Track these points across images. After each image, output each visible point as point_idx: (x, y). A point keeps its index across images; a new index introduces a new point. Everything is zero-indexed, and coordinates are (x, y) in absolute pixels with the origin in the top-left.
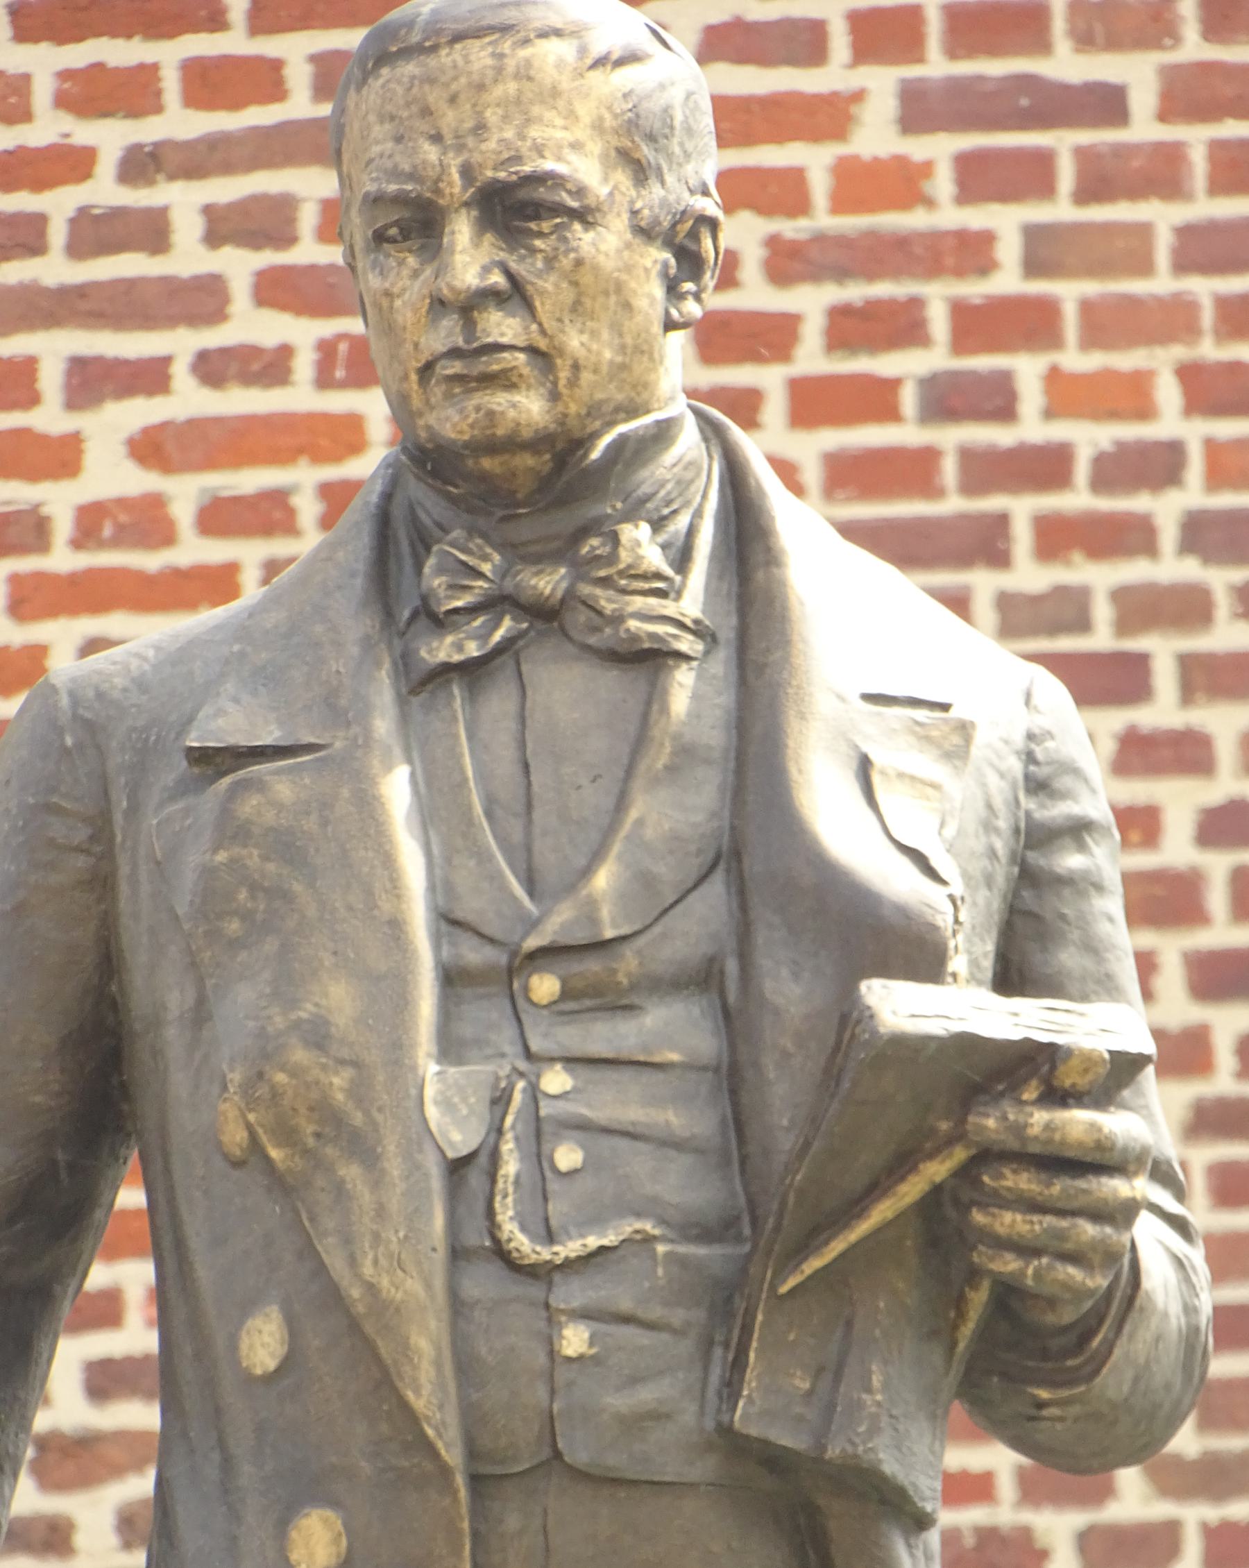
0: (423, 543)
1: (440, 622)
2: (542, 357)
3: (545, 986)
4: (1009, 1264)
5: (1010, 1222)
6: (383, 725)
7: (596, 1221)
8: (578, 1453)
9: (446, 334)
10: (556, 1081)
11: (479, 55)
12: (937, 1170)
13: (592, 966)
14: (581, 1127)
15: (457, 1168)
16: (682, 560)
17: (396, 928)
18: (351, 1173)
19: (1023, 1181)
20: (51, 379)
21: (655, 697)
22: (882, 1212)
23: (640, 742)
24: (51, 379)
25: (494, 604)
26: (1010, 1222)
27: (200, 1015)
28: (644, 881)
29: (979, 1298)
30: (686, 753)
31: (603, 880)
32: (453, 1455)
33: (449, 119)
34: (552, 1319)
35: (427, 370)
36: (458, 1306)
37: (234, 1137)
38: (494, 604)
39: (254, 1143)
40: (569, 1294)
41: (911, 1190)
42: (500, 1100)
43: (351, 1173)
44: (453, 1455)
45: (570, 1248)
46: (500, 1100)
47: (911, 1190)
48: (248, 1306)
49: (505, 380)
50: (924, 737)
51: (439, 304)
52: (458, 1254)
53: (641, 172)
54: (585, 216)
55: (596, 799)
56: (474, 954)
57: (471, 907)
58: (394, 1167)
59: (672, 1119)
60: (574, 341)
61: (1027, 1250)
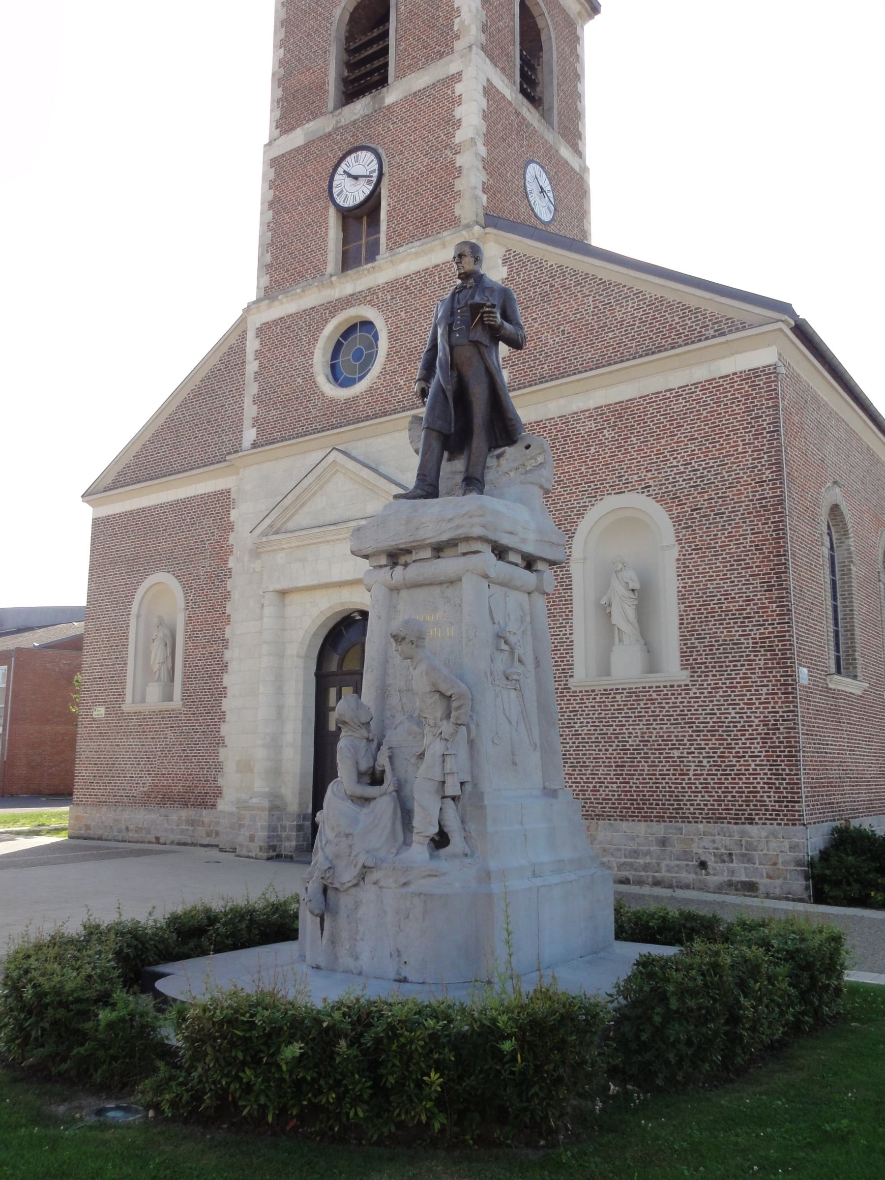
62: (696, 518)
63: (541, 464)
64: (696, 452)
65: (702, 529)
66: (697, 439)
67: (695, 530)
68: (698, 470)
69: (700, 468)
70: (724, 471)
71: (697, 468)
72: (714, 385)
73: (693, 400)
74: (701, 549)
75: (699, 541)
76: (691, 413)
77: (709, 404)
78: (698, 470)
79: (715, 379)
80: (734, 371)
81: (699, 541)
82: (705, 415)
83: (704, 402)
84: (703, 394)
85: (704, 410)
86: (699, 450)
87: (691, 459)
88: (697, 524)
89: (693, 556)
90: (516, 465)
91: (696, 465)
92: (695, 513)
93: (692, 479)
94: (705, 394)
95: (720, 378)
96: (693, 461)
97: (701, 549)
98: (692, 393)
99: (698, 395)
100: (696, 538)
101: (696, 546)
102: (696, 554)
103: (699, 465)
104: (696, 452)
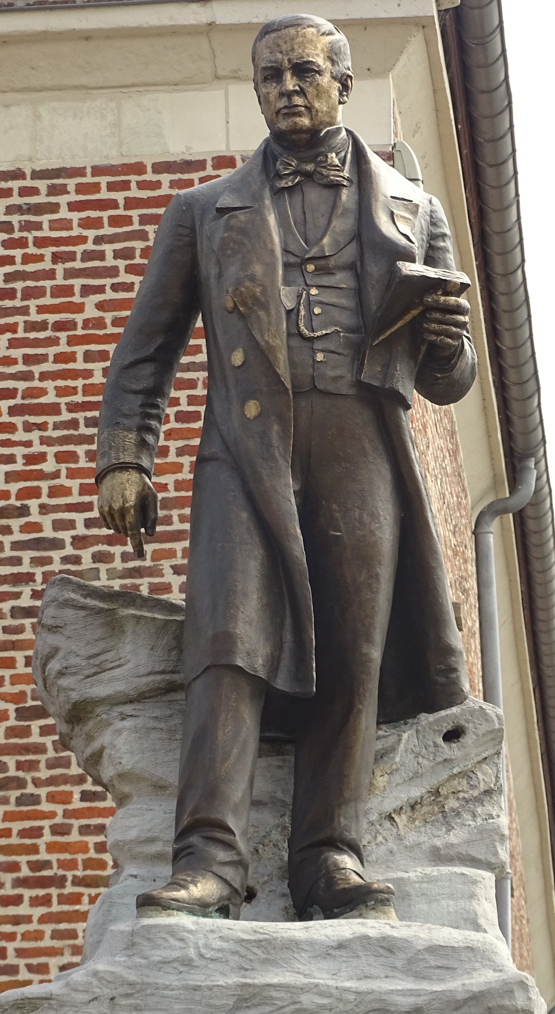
0: (275, 159)
1: (281, 177)
2: (309, 108)
3: (311, 267)
4: (434, 338)
5: (434, 326)
6: (268, 202)
7: (325, 328)
8: (320, 385)
9: (283, 102)
10: (314, 291)
11: (292, 31)
12: (415, 312)
13: (322, 262)
14: (321, 303)
15: (289, 312)
16: (343, 162)
17: (272, 252)
18: (262, 313)
19: (438, 315)
20: (77, 290)
21: (338, 196)
22: (400, 324)
23: (334, 207)
24: (77, 290)
25: (295, 173)
26: (434, 326)
27: (220, 276)
28: (335, 242)
29: (424, 348)
30: (346, 210)
31: (326, 241)
32: (289, 386)
33: (284, 47)
34: (314, 352)
35: (278, 112)
36: (289, 348)
37: (230, 305)
38: (295, 173)
39: (235, 306)
40: (318, 345)
41: (408, 318)
42: (300, 296)
43: (262, 313)
44: (289, 386)
45: (319, 334)
46: (300, 296)
47: (408, 318)
48: (233, 349)
49: (299, 114)
50: (406, 209)
51: (282, 95)
52: (289, 335)
53: (333, 62)
54: (320, 72)
55: (322, 222)
56: (292, 259)
57: (292, 248)
58: (273, 312)
59: (344, 302)
60: (317, 105)
61: (438, 334)
62: (40, 749)
63: (488, 792)
64: (49, 466)
65: (66, 798)
66: (54, 409)
67: (35, 800)
68: (57, 544)
69: (66, 536)
70: (166, 565)
71: (48, 533)
72: (135, 193)
73: (40, 243)
74: (60, 882)
75: (51, 848)
76: (28, 294)
77: (113, 272)
78: (57, 544)
79: (139, 168)
80: (221, 149)
81: (51, 848)
82: (91, 312)
83: (88, 256)
84: (86, 224)
85: (87, 290)
86: (60, 457)
87: (23, 494)
88: (44, 774)
89: (23, 909)
90: (416, 792)
91: (47, 521)
92: (35, 725)
93: (29, 578)
94: (96, 223)
95: (159, 168)
96: (33, 504)
97: (60, 882)
98: (38, 209)
99: (66, 224)
100: (37, 832)
101: (35, 866)
102: (35, 902)
103: (58, 525)
104: (49, 466)
